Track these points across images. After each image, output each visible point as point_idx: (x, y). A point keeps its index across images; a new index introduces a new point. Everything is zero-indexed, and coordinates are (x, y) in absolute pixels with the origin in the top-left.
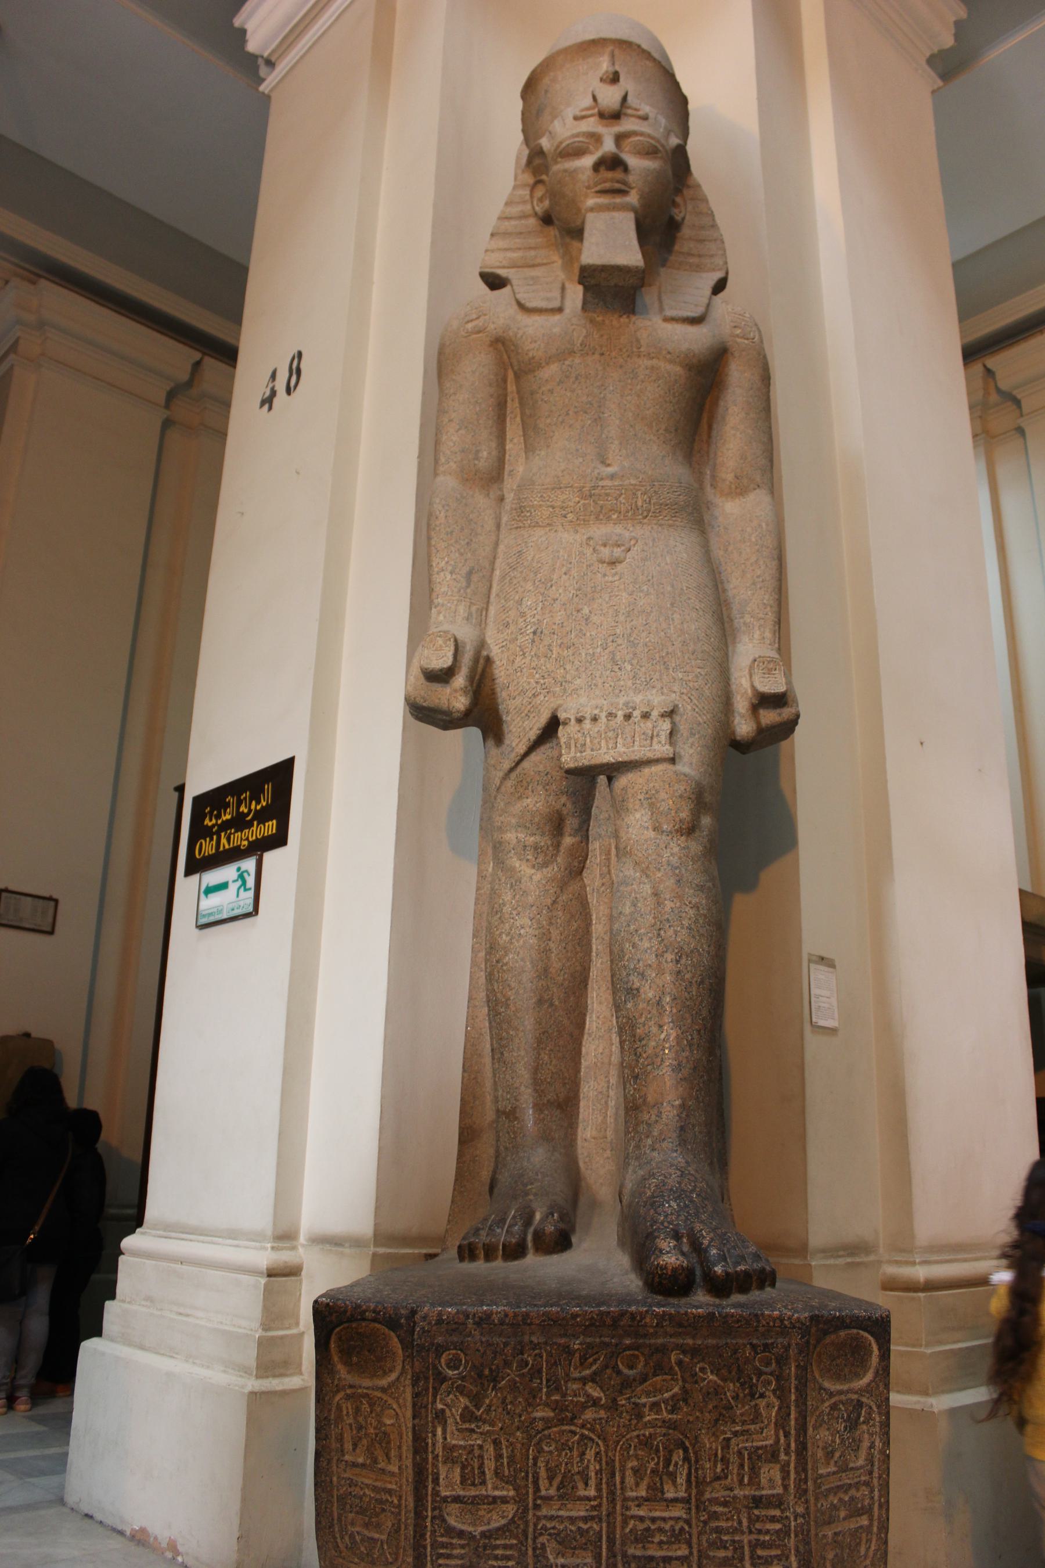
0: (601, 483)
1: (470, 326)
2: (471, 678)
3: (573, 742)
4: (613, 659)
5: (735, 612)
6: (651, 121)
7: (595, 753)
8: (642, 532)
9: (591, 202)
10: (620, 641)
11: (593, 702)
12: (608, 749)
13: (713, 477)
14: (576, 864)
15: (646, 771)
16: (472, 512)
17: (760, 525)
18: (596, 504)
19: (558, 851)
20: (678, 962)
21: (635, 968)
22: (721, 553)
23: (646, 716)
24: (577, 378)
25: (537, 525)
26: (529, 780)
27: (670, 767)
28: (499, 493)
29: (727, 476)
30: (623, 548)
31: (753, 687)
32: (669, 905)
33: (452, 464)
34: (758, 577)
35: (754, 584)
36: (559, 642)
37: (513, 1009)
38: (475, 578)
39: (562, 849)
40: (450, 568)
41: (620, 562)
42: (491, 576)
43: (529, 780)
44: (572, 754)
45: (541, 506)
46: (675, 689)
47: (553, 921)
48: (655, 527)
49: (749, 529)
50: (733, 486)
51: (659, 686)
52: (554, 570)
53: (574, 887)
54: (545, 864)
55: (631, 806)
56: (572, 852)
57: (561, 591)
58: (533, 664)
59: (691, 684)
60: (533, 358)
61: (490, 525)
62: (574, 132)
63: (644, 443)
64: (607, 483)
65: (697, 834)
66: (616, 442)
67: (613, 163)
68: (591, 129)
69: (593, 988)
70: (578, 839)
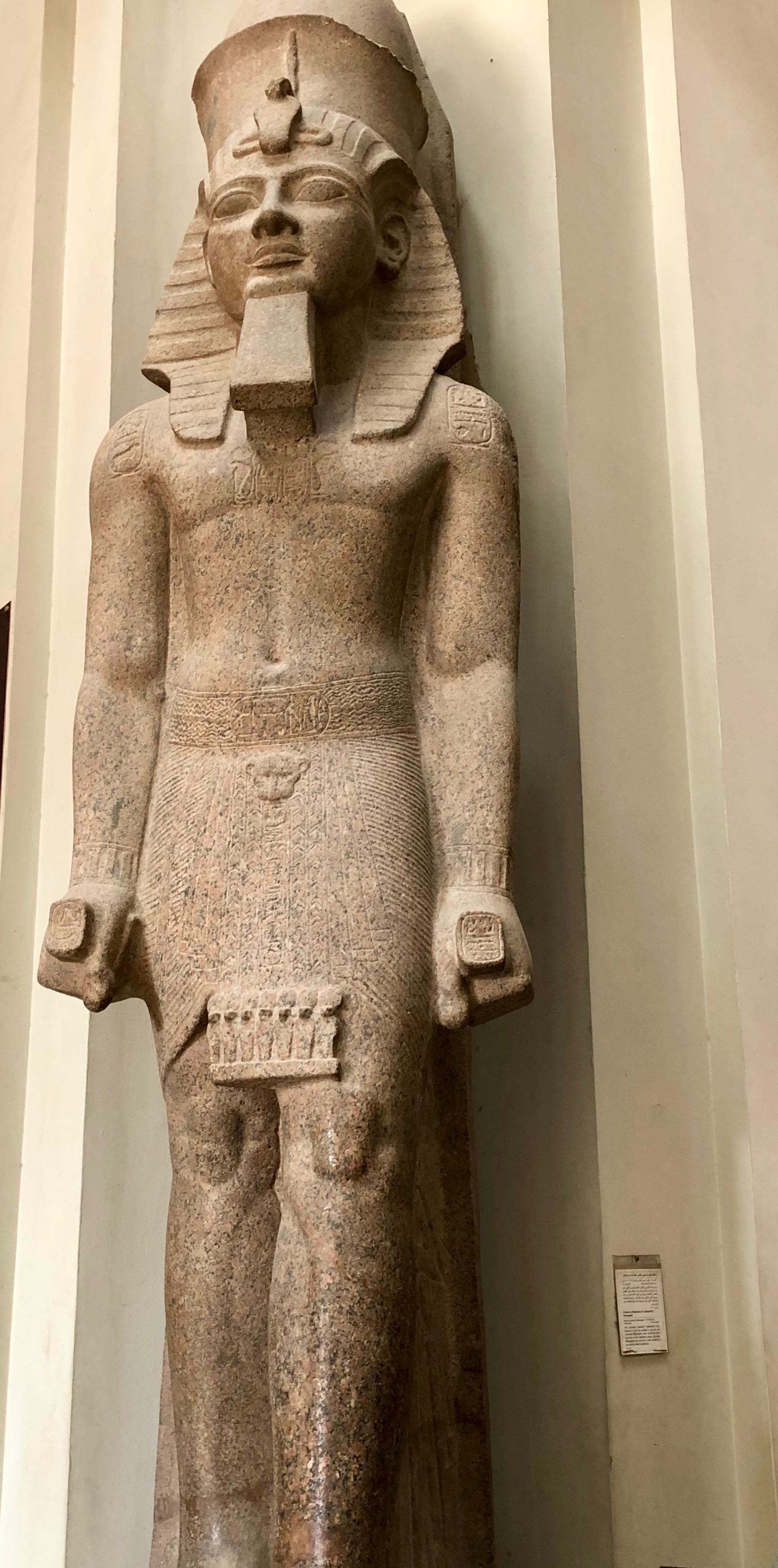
0: (264, 689)
1: (120, 460)
2: (109, 956)
3: (222, 1046)
4: (272, 932)
5: (447, 842)
6: (337, 143)
8: (320, 750)
9: (254, 281)
10: (281, 909)
11: (248, 994)
12: (260, 1059)
13: (431, 648)
14: (264, 1175)
15: (307, 1087)
16: (123, 722)
17: (485, 717)
18: (261, 716)
19: (238, 1162)
20: (332, 1361)
21: (286, 1363)
22: (434, 757)
23: (306, 1015)
24: (237, 540)
26: (195, 1073)
27: (335, 1084)
28: (159, 691)
29: (446, 647)
30: (290, 777)
32: (326, 1279)
36: (212, 907)
37: (190, 1367)
38: (124, 813)
39: (244, 1158)
40: (93, 803)
41: (285, 797)
42: (146, 807)
45: (196, 719)
46: (347, 973)
47: (235, 1252)
48: (334, 742)
49: (470, 723)
50: (454, 661)
52: (208, 808)
53: (264, 1203)
54: (223, 1179)
56: (256, 1160)
57: (215, 838)
58: (186, 934)
59: (368, 965)
60: (187, 512)
61: (146, 738)
62: (232, 178)
63: (322, 625)
64: (272, 688)
65: (371, 1173)
66: (286, 628)
67: (277, 224)
68: (251, 173)
70: (265, 1141)
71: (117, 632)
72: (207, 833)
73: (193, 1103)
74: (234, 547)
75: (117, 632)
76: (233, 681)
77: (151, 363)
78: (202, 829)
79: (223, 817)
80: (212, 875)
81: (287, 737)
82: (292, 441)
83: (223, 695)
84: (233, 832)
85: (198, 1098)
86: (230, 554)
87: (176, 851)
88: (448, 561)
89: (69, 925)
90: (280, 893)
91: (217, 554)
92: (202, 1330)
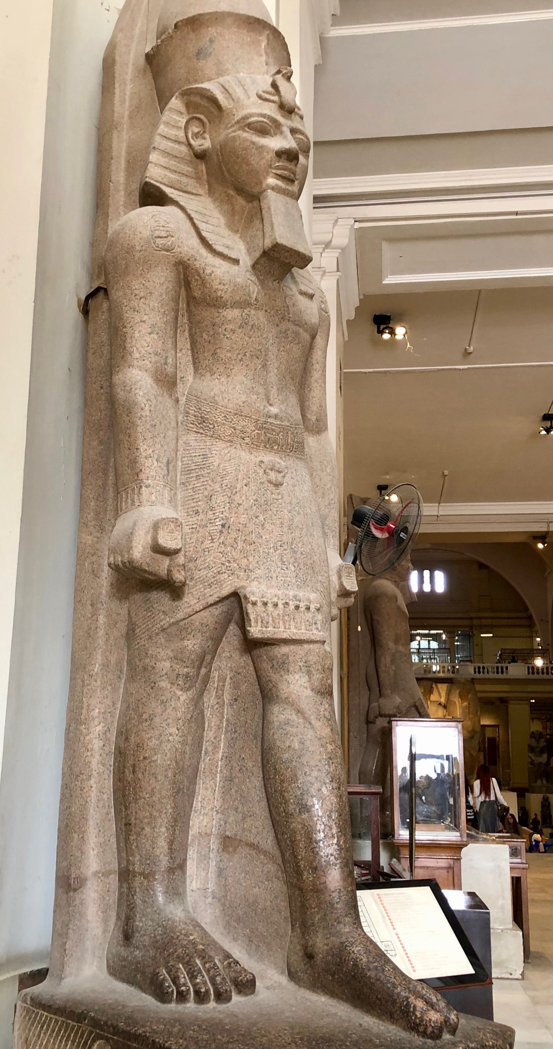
0: (269, 420)
3: (259, 618)
7: (276, 630)
10: (285, 547)
12: (285, 628)
25: (219, 438)
26: (193, 628)
31: (341, 584)
33: (147, 362)
34: (332, 500)
35: (329, 504)
36: (244, 538)
43: (193, 628)
44: (259, 628)
51: (310, 585)
55: (291, 669)
57: (243, 498)
69: (200, 778)
71: (159, 351)
72: (238, 494)
73: (186, 644)
74: (250, 330)
75: (159, 351)
76: (253, 410)
77: (152, 179)
78: (234, 491)
79: (248, 487)
80: (243, 519)
81: (277, 452)
82: (272, 279)
83: (246, 416)
84: (254, 498)
85: (189, 642)
86: (248, 334)
87: (213, 499)
88: (312, 372)
89: (173, 533)
90: (285, 538)
91: (241, 330)
92: (170, 775)
